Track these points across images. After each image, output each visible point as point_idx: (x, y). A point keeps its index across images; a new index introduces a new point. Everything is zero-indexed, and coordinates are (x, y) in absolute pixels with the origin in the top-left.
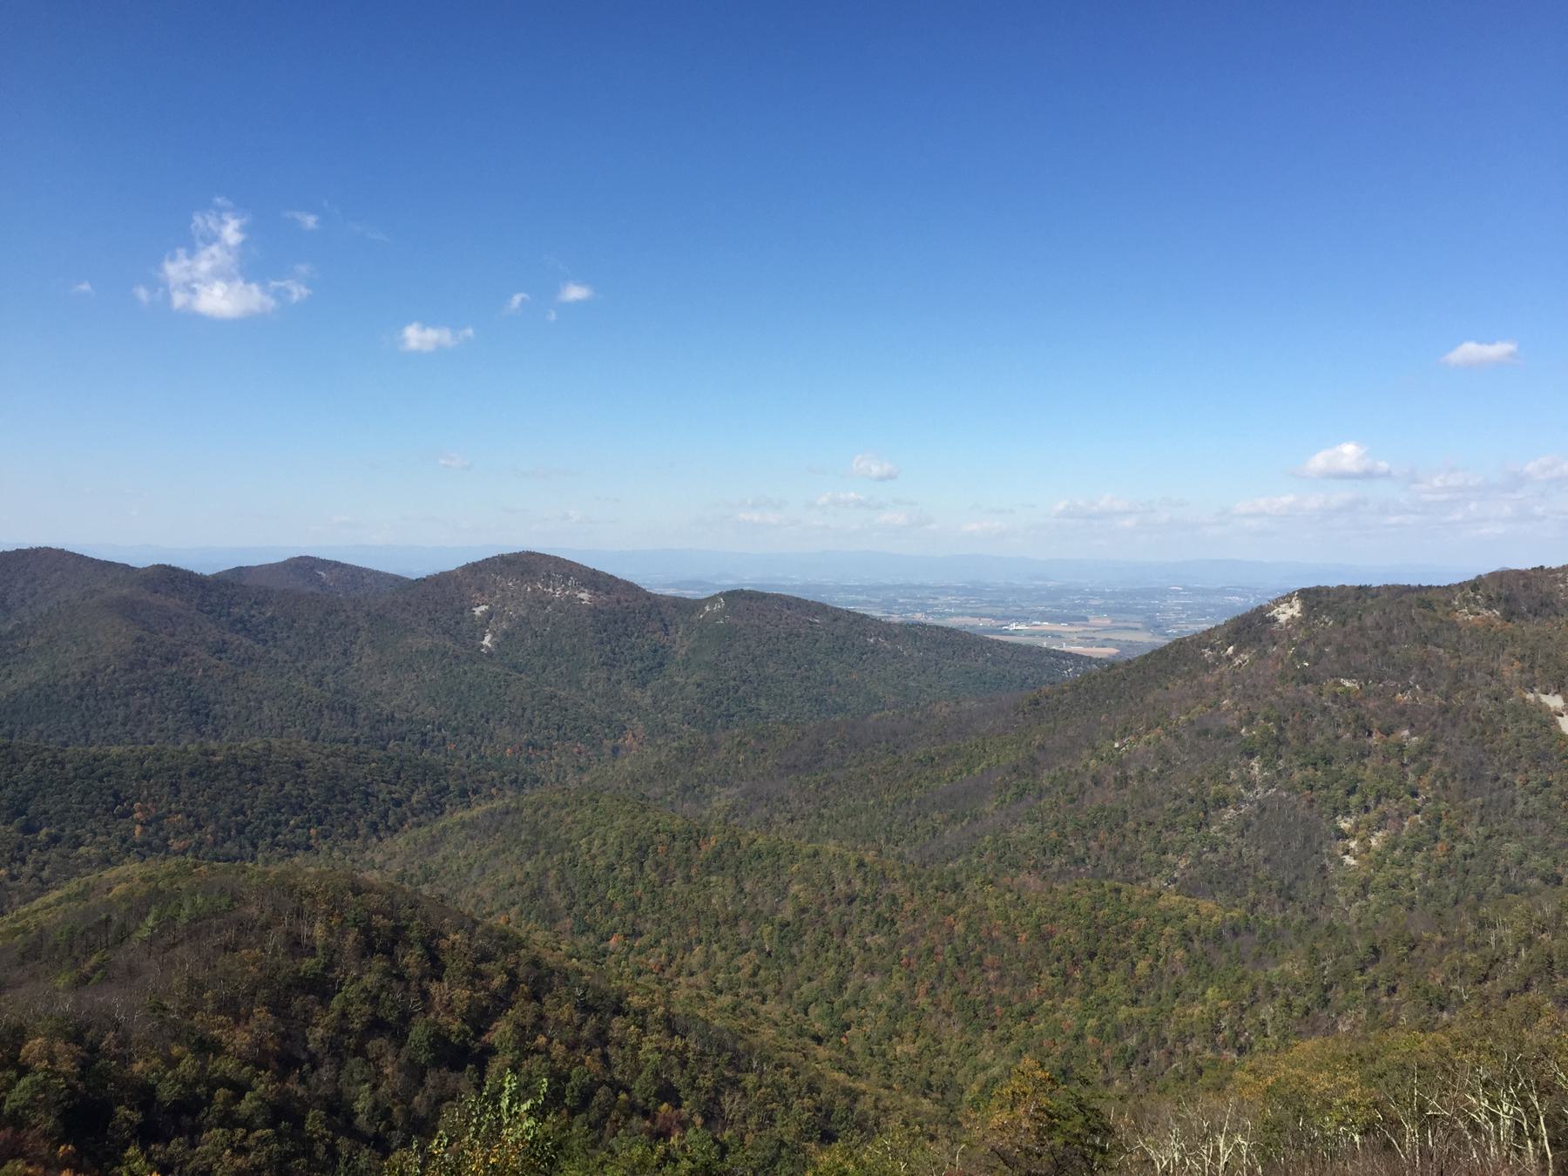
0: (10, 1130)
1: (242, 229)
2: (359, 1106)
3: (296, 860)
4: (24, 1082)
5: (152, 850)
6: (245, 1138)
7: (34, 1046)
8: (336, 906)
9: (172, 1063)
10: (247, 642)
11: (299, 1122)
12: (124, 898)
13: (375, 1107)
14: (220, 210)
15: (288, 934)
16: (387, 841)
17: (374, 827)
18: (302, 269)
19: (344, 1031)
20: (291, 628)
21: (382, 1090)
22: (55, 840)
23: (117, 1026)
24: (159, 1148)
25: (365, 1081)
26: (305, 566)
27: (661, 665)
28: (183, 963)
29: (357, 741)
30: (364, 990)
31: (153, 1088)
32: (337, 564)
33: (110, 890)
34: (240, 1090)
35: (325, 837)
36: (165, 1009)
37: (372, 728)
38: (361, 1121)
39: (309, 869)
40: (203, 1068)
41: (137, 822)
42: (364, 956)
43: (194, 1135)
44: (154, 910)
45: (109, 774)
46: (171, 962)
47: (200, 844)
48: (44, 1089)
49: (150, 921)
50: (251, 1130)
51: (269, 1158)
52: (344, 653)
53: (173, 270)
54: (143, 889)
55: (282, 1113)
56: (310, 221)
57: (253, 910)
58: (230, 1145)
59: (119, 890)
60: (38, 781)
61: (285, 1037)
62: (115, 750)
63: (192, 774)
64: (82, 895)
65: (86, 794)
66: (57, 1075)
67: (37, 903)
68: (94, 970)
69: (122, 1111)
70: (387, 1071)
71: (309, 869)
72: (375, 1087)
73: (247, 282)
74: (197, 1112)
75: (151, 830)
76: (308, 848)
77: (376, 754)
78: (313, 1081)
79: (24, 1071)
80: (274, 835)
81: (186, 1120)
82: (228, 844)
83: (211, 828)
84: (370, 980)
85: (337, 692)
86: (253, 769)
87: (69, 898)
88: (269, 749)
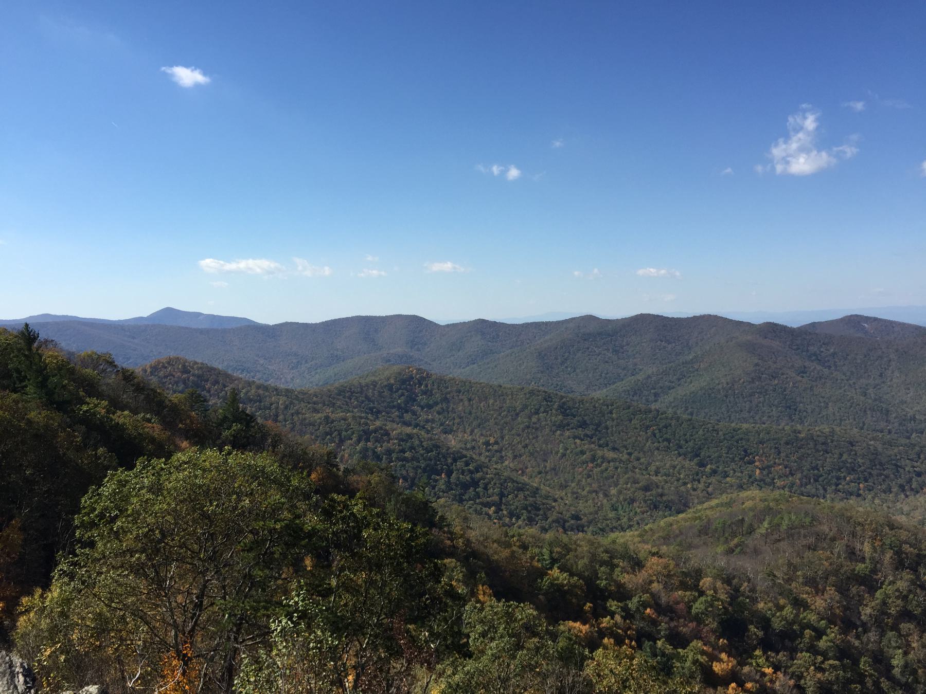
0: (695, 623)
1: (817, 120)
2: (895, 662)
3: (851, 502)
4: (703, 599)
5: (766, 484)
6: (823, 662)
7: (706, 582)
8: (877, 534)
9: (780, 608)
10: (819, 368)
11: (856, 662)
12: (751, 509)
13: (906, 666)
14: (804, 111)
15: (847, 546)
16: (911, 498)
17: (902, 487)
18: (855, 137)
19: (884, 613)
20: (846, 359)
21: (911, 656)
22: (714, 472)
23: (749, 581)
24: (773, 655)
25: (899, 648)
26: (854, 321)
28: (784, 552)
29: (890, 432)
30: (898, 590)
31: (769, 620)
32: (875, 319)
33: (743, 503)
34: (819, 633)
35: (870, 490)
36: (775, 576)
37: (900, 424)
38: (896, 672)
39: (860, 508)
40: (797, 615)
41: (757, 467)
42: (897, 569)
43: (793, 653)
44: (768, 519)
45: (741, 439)
46: (778, 550)
47: (792, 485)
48: (712, 606)
49: (766, 524)
50: (826, 658)
51: (837, 678)
52: (881, 375)
53: (777, 152)
54: (762, 505)
55: (844, 653)
56: (859, 106)
57: (825, 528)
58: (814, 664)
59: (749, 504)
60: (706, 439)
61: (846, 608)
63: (787, 443)
64: (729, 504)
65: (729, 448)
66: (718, 600)
67: (706, 505)
68: (736, 546)
69: (752, 628)
70: (914, 645)
71: (860, 508)
72: (906, 653)
73: (819, 151)
74: (795, 640)
75: (765, 473)
76: (859, 495)
77: (904, 441)
78: (865, 639)
79: (702, 593)
80: (837, 485)
81: (787, 643)
83: (799, 475)
84: (902, 585)
85: (875, 400)
86: (823, 444)
87: (722, 505)
88: (833, 432)
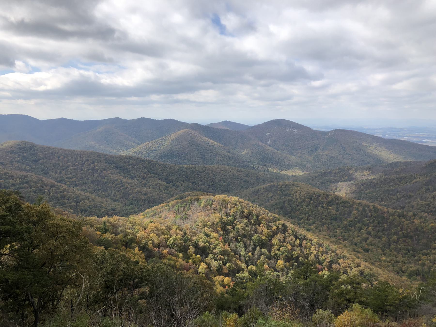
26: (226, 123)
27: (316, 149)
62: (186, 166)
82: (210, 189)
